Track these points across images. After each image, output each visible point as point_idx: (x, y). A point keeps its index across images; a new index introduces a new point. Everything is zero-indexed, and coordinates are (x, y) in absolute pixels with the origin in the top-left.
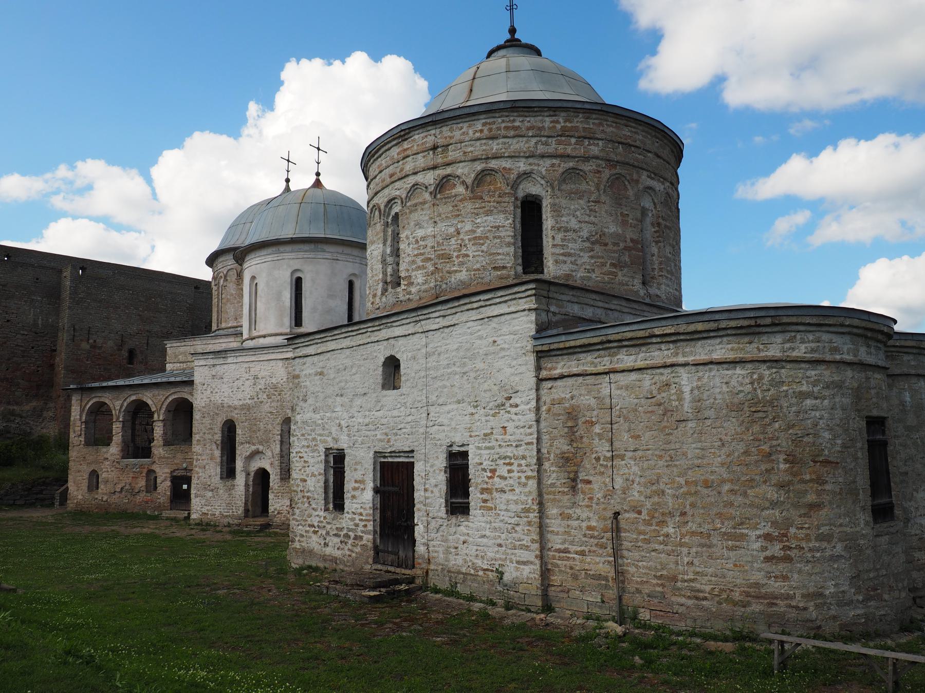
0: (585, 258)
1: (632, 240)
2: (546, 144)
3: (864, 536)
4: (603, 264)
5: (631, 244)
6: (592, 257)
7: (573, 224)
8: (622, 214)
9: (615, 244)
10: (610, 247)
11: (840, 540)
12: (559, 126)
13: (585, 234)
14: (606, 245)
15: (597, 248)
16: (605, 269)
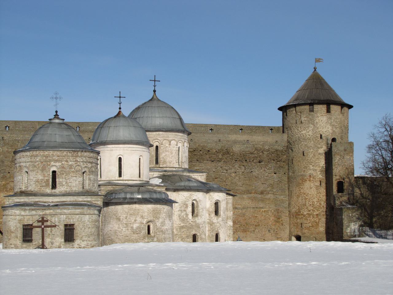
0: (34, 185)
1: (46, 180)
2: (28, 159)
3: (18, 244)
4: (38, 187)
5: (46, 181)
6: (35, 185)
7: (32, 178)
8: (44, 174)
9: (41, 182)
10: (40, 182)
11: (13, 245)
12: (31, 155)
13: (34, 180)
14: (39, 182)
15: (37, 183)
16: (39, 188)
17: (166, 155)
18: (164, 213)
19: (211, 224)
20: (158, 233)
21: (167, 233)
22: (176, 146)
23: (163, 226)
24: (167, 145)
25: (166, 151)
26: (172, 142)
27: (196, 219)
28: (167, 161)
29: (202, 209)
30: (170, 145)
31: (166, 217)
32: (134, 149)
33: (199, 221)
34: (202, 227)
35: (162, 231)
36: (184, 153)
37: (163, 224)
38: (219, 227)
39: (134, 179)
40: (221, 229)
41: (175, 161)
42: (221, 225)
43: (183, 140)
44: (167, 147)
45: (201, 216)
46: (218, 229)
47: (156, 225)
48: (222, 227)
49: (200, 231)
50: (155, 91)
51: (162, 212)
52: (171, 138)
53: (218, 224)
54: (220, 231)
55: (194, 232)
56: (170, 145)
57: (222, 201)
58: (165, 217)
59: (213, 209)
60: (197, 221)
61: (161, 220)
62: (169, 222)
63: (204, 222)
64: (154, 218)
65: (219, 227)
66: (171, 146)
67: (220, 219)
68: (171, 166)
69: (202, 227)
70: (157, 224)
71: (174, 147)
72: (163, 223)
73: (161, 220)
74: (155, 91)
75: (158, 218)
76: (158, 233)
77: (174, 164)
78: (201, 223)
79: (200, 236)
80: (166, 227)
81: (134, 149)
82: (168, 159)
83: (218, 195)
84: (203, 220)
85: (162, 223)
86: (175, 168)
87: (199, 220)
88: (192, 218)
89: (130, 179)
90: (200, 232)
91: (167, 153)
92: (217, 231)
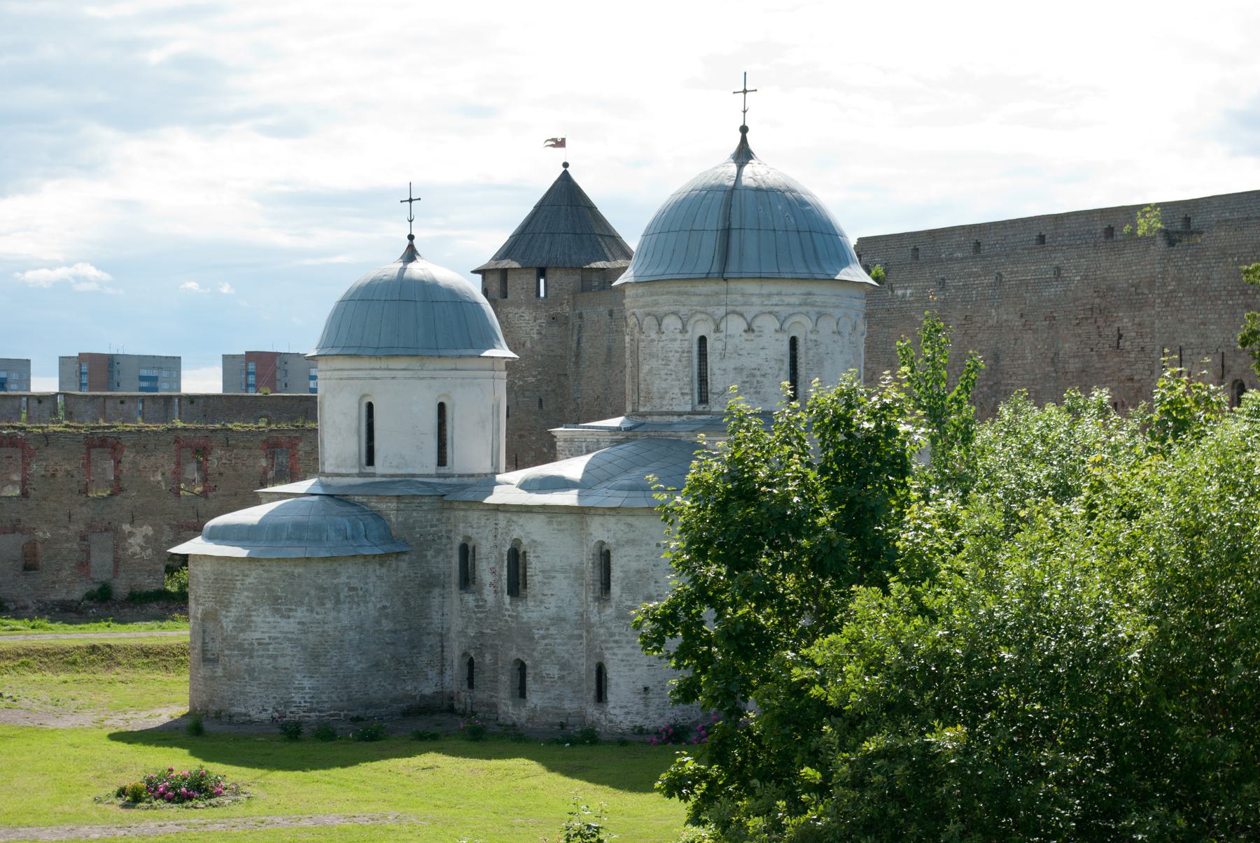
17: (650, 371)
18: (247, 590)
19: (589, 626)
20: (227, 652)
21: (261, 653)
22: (679, 336)
23: (243, 630)
24: (654, 335)
25: (652, 356)
26: (666, 321)
27: (520, 609)
28: (655, 389)
29: (543, 572)
30: (660, 332)
31: (254, 603)
32: (345, 374)
33: (530, 614)
34: (544, 637)
35: (240, 647)
36: (723, 357)
37: (244, 623)
38: (605, 641)
39: (343, 471)
40: (612, 648)
41: (677, 391)
42: (612, 635)
43: (722, 310)
44: (653, 341)
45: (540, 597)
46: (603, 646)
47: (222, 627)
48: (616, 642)
49: (533, 650)
50: (744, 130)
51: (238, 585)
52: (666, 308)
53: (602, 631)
54: (607, 655)
55: (514, 654)
56: (660, 332)
57: (619, 544)
58: (249, 602)
59: (591, 574)
60: (524, 615)
61: (234, 612)
62: (271, 619)
63: (558, 620)
64: (216, 602)
65: (605, 641)
66: (664, 337)
67: (610, 611)
68: (664, 409)
69: (544, 637)
70: (225, 622)
71: (675, 340)
72: (242, 622)
73: (234, 612)
74: (744, 130)
75: (227, 606)
76: (227, 652)
77: (675, 402)
78: (539, 622)
79: (535, 667)
80: (257, 635)
81: (345, 374)
82: (657, 385)
83: (602, 525)
84: (552, 611)
85: (238, 620)
86: (680, 414)
87: (530, 612)
88: (511, 604)
89: (336, 471)
90: (535, 654)
91: (654, 363)
92: (601, 655)
